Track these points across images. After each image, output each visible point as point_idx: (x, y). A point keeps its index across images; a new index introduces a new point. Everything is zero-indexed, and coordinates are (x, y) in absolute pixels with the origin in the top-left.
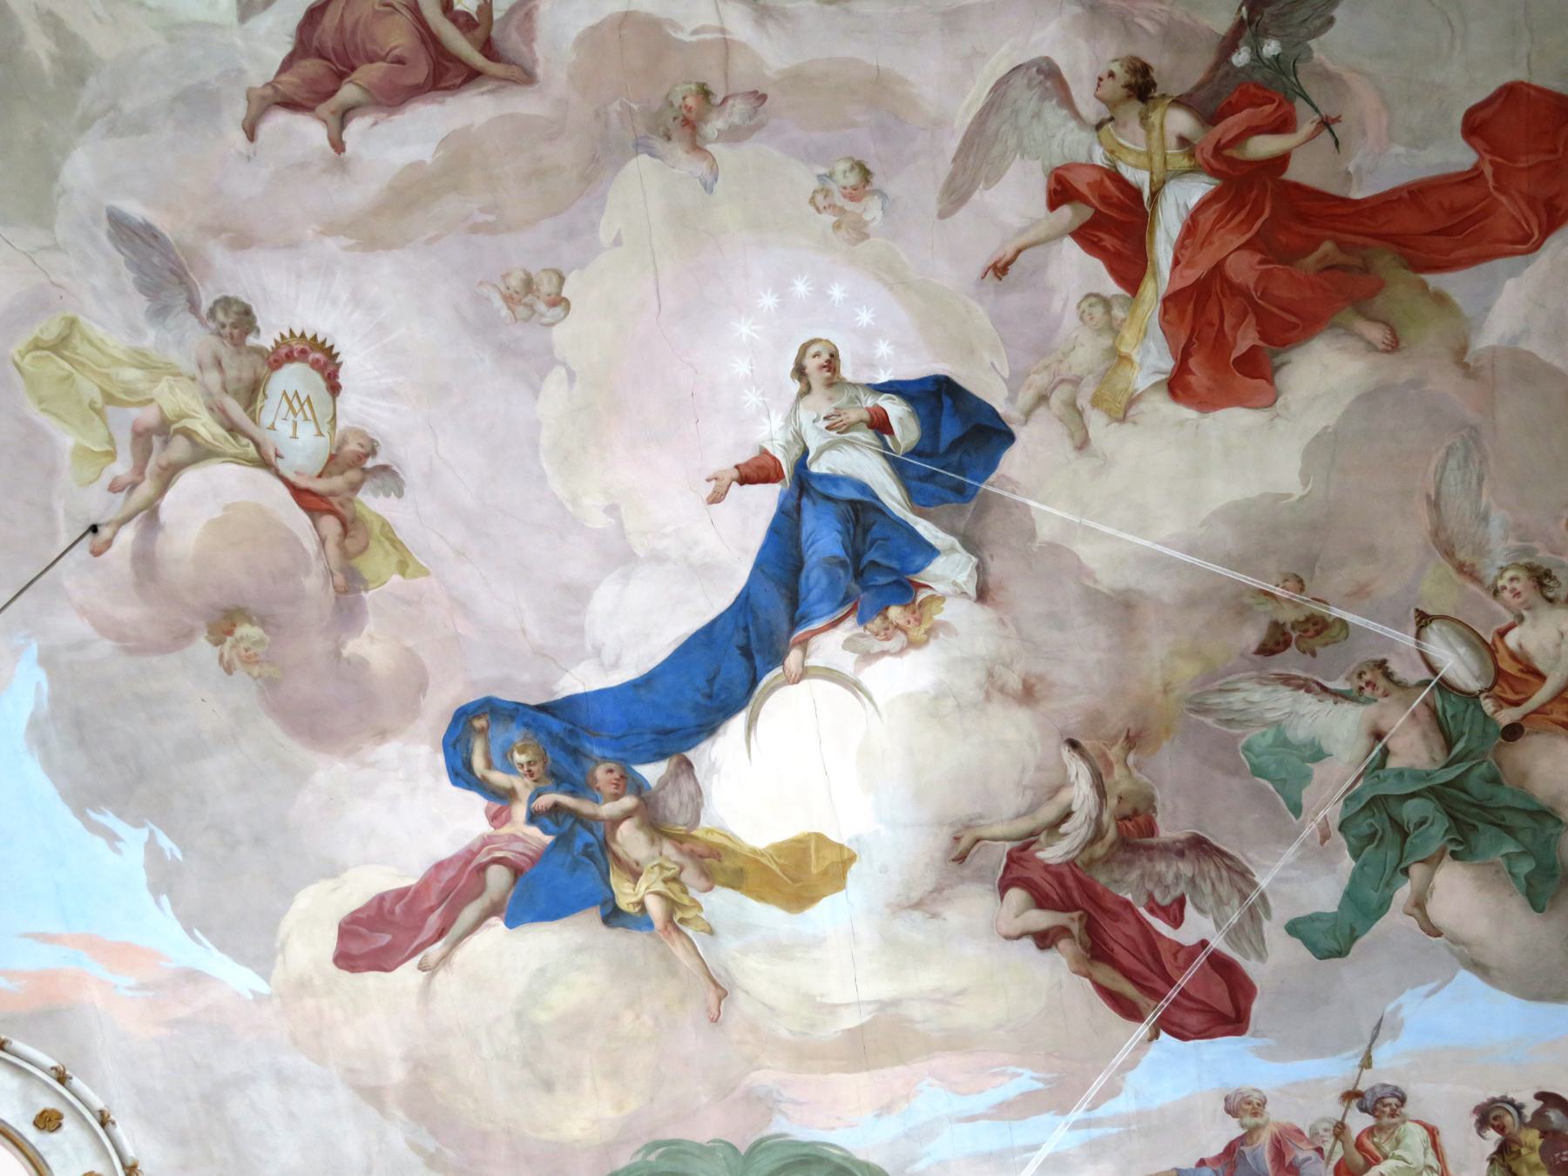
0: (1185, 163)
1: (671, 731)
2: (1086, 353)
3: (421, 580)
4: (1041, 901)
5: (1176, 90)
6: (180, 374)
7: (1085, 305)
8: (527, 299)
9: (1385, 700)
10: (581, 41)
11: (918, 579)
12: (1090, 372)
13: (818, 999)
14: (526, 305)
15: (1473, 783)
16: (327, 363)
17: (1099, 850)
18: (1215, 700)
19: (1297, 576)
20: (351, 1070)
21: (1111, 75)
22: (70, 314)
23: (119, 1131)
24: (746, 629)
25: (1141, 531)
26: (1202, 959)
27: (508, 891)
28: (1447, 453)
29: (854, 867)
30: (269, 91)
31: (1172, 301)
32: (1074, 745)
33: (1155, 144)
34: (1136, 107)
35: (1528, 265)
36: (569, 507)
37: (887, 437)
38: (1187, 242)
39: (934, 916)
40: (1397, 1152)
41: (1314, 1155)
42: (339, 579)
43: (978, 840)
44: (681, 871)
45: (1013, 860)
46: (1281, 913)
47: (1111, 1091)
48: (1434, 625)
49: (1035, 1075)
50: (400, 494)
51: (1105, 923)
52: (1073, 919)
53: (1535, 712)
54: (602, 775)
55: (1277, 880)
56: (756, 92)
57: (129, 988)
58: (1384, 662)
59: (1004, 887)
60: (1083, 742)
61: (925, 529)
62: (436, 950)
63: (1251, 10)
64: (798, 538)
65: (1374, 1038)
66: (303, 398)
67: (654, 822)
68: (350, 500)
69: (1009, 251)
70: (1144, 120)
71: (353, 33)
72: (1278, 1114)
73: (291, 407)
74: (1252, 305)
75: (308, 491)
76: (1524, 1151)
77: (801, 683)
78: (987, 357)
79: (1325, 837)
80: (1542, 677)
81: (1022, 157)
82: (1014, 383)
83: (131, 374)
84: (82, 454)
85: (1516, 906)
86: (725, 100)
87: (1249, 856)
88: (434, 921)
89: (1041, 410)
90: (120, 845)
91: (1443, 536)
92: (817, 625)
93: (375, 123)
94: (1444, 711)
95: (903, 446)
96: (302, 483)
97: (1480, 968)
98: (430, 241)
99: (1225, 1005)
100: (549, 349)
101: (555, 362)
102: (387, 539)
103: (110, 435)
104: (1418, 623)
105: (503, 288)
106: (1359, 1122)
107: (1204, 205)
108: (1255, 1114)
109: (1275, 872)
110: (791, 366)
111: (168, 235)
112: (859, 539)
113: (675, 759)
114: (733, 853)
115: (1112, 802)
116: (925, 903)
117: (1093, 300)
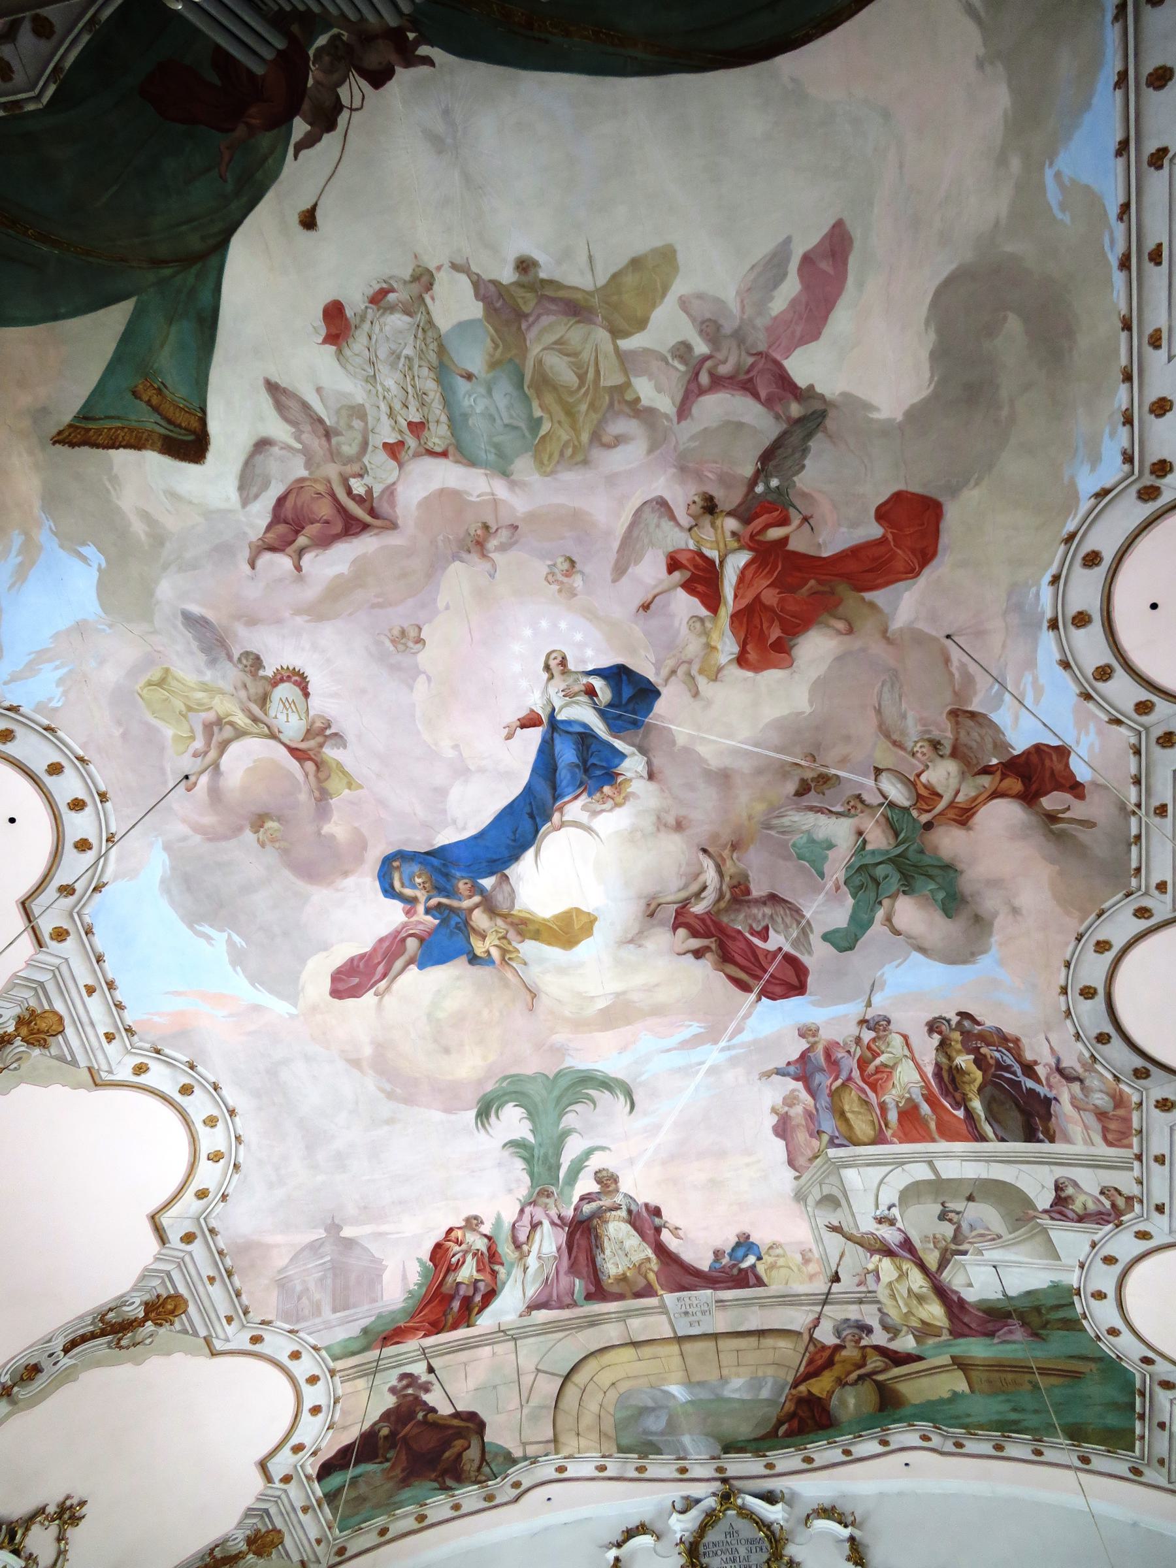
0: (736, 545)
2: (693, 647)
3: (360, 791)
4: (695, 934)
5: (728, 507)
7: (691, 622)
8: (403, 641)
9: (861, 815)
10: (420, 504)
11: (618, 770)
12: (696, 657)
15: (911, 854)
16: (301, 681)
17: (722, 904)
18: (775, 822)
20: (343, 1051)
21: (694, 502)
22: (165, 666)
23: (224, 1092)
24: (531, 804)
25: (729, 736)
26: (780, 957)
29: (597, 924)
30: (260, 543)
31: (735, 617)
32: (705, 851)
33: (720, 537)
34: (707, 520)
35: (914, 584)
36: (434, 747)
38: (741, 585)
41: (846, 1054)
42: (317, 794)
43: (659, 905)
44: (507, 932)
45: (678, 913)
47: (739, 1030)
48: (883, 774)
50: (345, 747)
51: (729, 943)
53: (940, 814)
54: (462, 886)
55: (815, 912)
58: (860, 795)
59: (675, 928)
60: (710, 849)
61: (618, 744)
62: (383, 984)
63: (762, 464)
65: (872, 991)
67: (491, 910)
68: (319, 752)
69: (650, 597)
70: (713, 525)
71: (302, 506)
72: (826, 1035)
73: (285, 706)
75: (297, 749)
77: (562, 829)
78: (643, 653)
79: (838, 888)
80: (941, 796)
82: (658, 666)
83: (200, 695)
84: (177, 738)
85: (938, 917)
86: (497, 530)
87: (799, 902)
88: (380, 969)
89: (673, 678)
90: (213, 942)
91: (883, 727)
92: (566, 799)
93: (317, 556)
96: (294, 745)
97: (922, 950)
98: (350, 614)
99: (794, 980)
100: (417, 666)
101: (419, 672)
103: (191, 727)
106: (867, 1036)
108: (814, 1036)
110: (542, 665)
112: (585, 752)
113: (499, 875)
114: (533, 921)
115: (727, 879)
116: (634, 940)
117: (694, 619)
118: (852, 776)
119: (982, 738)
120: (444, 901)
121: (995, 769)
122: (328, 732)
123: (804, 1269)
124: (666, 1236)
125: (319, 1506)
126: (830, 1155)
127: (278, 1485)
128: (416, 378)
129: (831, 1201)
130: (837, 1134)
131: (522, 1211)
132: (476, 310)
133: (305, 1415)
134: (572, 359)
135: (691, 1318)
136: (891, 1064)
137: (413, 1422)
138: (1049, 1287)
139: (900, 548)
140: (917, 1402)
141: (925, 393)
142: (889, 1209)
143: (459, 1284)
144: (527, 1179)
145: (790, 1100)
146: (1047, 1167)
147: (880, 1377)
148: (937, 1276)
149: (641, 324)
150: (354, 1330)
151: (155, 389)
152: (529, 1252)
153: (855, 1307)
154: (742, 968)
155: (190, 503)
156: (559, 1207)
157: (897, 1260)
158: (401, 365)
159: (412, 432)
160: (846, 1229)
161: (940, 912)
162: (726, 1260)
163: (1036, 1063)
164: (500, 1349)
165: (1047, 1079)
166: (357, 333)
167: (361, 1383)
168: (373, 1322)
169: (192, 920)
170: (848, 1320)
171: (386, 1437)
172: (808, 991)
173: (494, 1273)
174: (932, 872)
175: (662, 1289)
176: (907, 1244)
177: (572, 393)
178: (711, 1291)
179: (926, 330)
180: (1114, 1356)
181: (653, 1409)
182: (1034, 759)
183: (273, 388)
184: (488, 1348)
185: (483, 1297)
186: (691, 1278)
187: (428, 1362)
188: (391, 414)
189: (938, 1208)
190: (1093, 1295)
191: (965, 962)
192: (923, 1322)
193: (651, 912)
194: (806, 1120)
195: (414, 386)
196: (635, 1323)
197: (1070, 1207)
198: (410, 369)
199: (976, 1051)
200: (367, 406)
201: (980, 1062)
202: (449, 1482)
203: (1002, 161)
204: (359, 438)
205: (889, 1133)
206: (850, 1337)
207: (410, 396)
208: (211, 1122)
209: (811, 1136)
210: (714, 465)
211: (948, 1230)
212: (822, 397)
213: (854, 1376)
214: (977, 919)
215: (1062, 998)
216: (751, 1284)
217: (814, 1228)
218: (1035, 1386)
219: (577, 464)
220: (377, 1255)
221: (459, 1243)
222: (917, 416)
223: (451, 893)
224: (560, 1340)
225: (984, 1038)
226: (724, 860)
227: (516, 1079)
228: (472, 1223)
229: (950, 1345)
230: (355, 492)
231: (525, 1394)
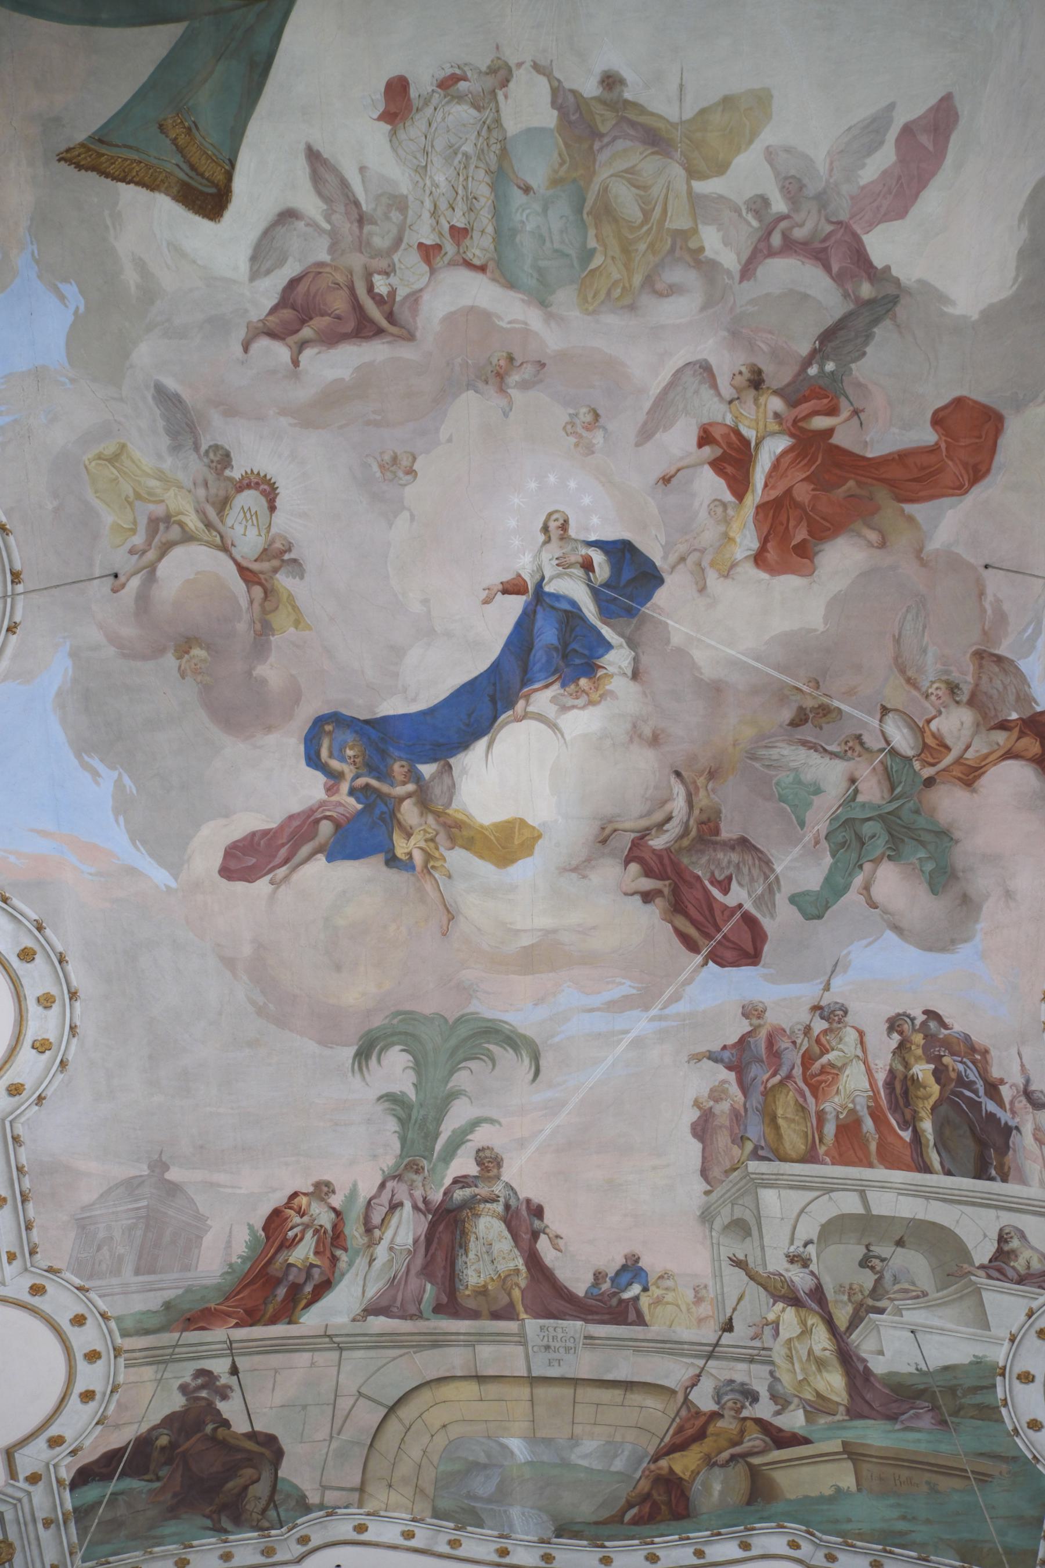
0: (776, 428)
2: (710, 535)
3: (307, 632)
4: (648, 873)
5: (776, 385)
6: (182, 488)
7: (712, 506)
8: (392, 469)
11: (599, 662)
13: (509, 926)
14: (391, 472)
16: (270, 492)
17: (686, 842)
18: (762, 752)
19: (816, 680)
21: (741, 373)
23: (70, 968)
24: (494, 684)
26: (738, 915)
27: (330, 838)
28: (907, 611)
29: (540, 842)
30: (260, 325)
31: (761, 508)
32: (678, 774)
33: (761, 415)
34: (752, 393)
37: (591, 574)
38: (773, 474)
39: (584, 877)
40: (840, 1046)
41: (790, 1045)
42: (258, 626)
43: (615, 831)
44: (437, 834)
45: (635, 844)
46: (787, 889)
47: (676, 998)
48: (890, 715)
49: (632, 984)
50: (302, 578)
51: (684, 889)
52: (665, 885)
53: (944, 770)
54: (398, 769)
56: (540, 362)
57: (91, 874)
58: (861, 735)
59: (627, 862)
60: (684, 773)
61: (607, 632)
62: (282, 872)
63: (821, 343)
64: (532, 630)
65: (833, 972)
66: (253, 512)
68: (271, 578)
69: (673, 470)
70: (756, 400)
72: (773, 1018)
75: (248, 569)
76: (913, 1047)
77: (523, 721)
79: (817, 843)
80: (948, 749)
81: (686, 416)
82: (667, 548)
83: (153, 483)
85: (922, 890)
86: (522, 364)
88: (283, 852)
89: (681, 566)
90: (99, 780)
91: (900, 661)
93: (319, 353)
94: (892, 768)
95: (599, 580)
96: (245, 563)
97: (897, 929)
99: (749, 948)
102: (290, 604)
103: (135, 518)
104: (882, 713)
105: (379, 459)
106: (819, 1025)
107: (784, 453)
108: (759, 1018)
109: (785, 863)
110: (541, 525)
111: (188, 402)
113: (442, 762)
114: (469, 827)
115: (696, 812)
116: (579, 869)
117: (717, 503)
118: (855, 713)
119: (1005, 688)
120: (374, 783)
121: (1012, 725)
122: (286, 557)
123: (694, 1309)
124: (543, 1244)
125: (65, 1523)
126: (750, 1169)
127: (22, 1484)
128: (470, 179)
129: (741, 1228)
130: (763, 1144)
131: (383, 1185)
132: (549, 118)
133: (74, 1398)
134: (642, 193)
135: (552, 1355)
136: (839, 1064)
137: (199, 1435)
138: (971, 1363)
139: (952, 460)
140: (792, 1497)
141: (1005, 294)
142: (805, 1246)
143: (290, 1265)
144: (397, 1145)
145: (717, 1094)
146: (992, 1212)
147: (756, 1461)
148: (845, 1337)
149: (721, 168)
150: (154, 1301)
151: (184, 127)
152: (381, 1239)
153: (742, 1366)
154: (694, 922)
155: (194, 262)
156: (427, 1188)
157: (803, 1312)
158: (456, 162)
159: (452, 236)
160: (751, 1265)
161: (925, 886)
162: (606, 1286)
163: (1002, 1082)
164: (320, 1358)
165: (1012, 1103)
166: (417, 117)
167: (148, 1373)
168: (178, 1297)
169: (82, 747)
170: (732, 1381)
171: (163, 1449)
172: (762, 962)
173: (334, 1260)
174: (927, 837)
175: (526, 1312)
176: (818, 1294)
179: (1019, 227)
180: (1030, 1457)
181: (485, 1467)
183: (313, 156)
184: (307, 1356)
185: (316, 1287)
186: (563, 1303)
187: (233, 1360)
188: (434, 213)
189: (860, 1251)
190: (1019, 1377)
191: (943, 949)
192: (819, 1395)
193: (604, 839)
194: (731, 1120)
195: (465, 188)
196: (485, 1351)
197: (1012, 1264)
198: (465, 167)
199: (937, 1060)
200: (411, 198)
201: (939, 1074)
202: (226, 1523)
204: (394, 231)
205: (822, 1150)
206: (730, 1404)
207: (459, 198)
208: (46, 1001)
209: (733, 1142)
210: (769, 336)
211: (868, 1280)
212: (897, 282)
213: (726, 1455)
216: (630, 1320)
217: (716, 1260)
218: (934, 1489)
219: (623, 307)
220: (201, 1210)
221: (301, 1213)
223: (385, 775)
224: (394, 1359)
225: (947, 1044)
226: (697, 788)
227: (410, 1016)
228: (322, 1190)
229: (845, 1428)
230: (376, 290)
231: (338, 1422)
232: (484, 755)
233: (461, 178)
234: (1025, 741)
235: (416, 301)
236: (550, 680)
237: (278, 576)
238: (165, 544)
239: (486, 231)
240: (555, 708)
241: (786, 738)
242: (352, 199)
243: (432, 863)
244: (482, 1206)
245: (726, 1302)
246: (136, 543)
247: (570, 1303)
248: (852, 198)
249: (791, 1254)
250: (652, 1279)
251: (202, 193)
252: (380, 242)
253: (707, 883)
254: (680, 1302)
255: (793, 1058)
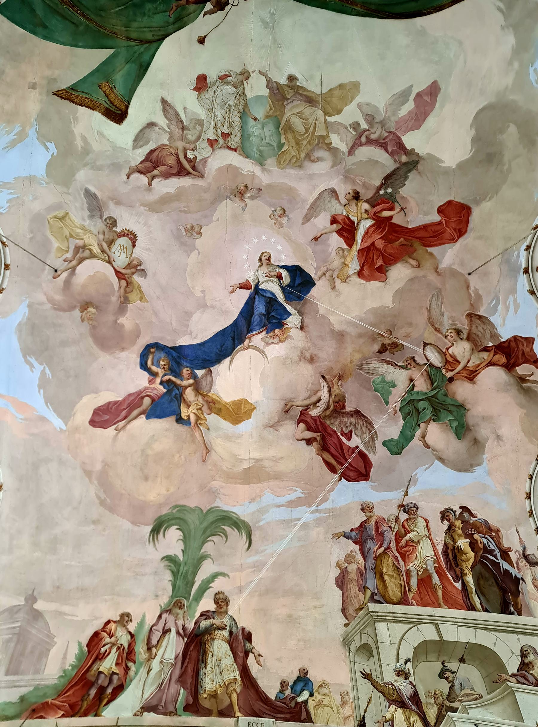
0: (366, 216)
1: (208, 360)
2: (337, 263)
4: (309, 429)
9: (414, 369)
10: (217, 170)
11: (284, 322)
13: (237, 456)
15: (440, 396)
16: (133, 238)
17: (328, 413)
20: (84, 463)
21: (349, 193)
24: (234, 332)
25: (347, 314)
26: (356, 452)
27: (149, 407)
28: (433, 296)
31: (360, 251)
32: (323, 377)
33: (359, 211)
34: (355, 201)
35: (454, 246)
39: (276, 430)
40: (415, 529)
42: (122, 299)
43: (292, 406)
44: (203, 406)
47: (325, 500)
48: (428, 346)
49: (301, 491)
50: (145, 278)
51: (328, 438)
52: (318, 436)
53: (457, 373)
54: (185, 372)
57: (21, 419)
58: (414, 357)
59: (298, 423)
61: (288, 307)
62: (122, 424)
63: (385, 181)
64: (253, 306)
65: (409, 485)
67: (197, 390)
70: (356, 205)
72: (378, 512)
74: (381, 253)
75: (120, 272)
76: (456, 529)
79: (395, 413)
80: (460, 363)
82: (317, 269)
83: (79, 231)
84: (59, 249)
85: (452, 437)
86: (251, 189)
87: (372, 418)
88: (124, 413)
89: (324, 277)
90: (34, 369)
91: (431, 320)
92: (254, 333)
94: (431, 373)
96: (118, 269)
97: (441, 459)
98: (168, 212)
99: (363, 470)
102: (139, 289)
104: (424, 346)
106: (403, 516)
107: (370, 227)
108: (370, 512)
112: (270, 308)
113: (207, 369)
114: (219, 403)
115: (333, 397)
116: (274, 426)
118: (410, 346)
119: (484, 331)
120: (173, 378)
121: (490, 348)
122: (139, 268)
124: (251, 660)
128: (231, 114)
131: (160, 617)
132: (266, 92)
134: (305, 121)
136: (416, 541)
139: (449, 228)
142: (406, 663)
143: (100, 673)
145: (349, 559)
149: (339, 112)
151: (110, 87)
152: (156, 655)
154: (333, 456)
155: (108, 140)
156: (186, 619)
157: (408, 712)
158: (225, 108)
160: (374, 677)
161: (454, 435)
163: (510, 549)
165: (517, 563)
169: (26, 352)
172: (370, 479)
173: (127, 669)
174: (452, 408)
175: (240, 711)
176: (415, 697)
177: (301, 135)
178: (273, 720)
182: (513, 344)
183: (164, 102)
189: (439, 667)
191: (467, 470)
200: (205, 121)
201: (473, 545)
203: (510, 63)
204: (198, 133)
205: (410, 596)
211: (444, 687)
212: (418, 155)
214: (476, 442)
215: (527, 502)
217: (353, 673)
221: (111, 635)
222: (462, 166)
223: (179, 375)
226: (333, 384)
227: (182, 508)
230: (188, 157)
232: (228, 367)
233: (227, 114)
234: (497, 357)
235: (205, 162)
236: (261, 330)
237: (134, 276)
238: (81, 258)
239: (237, 135)
240: (263, 343)
241: (377, 359)
242: (180, 120)
243: (199, 422)
244: (216, 632)
245: (360, 704)
246: (68, 257)
247: (266, 704)
248: (396, 122)
249: (398, 669)
250: (315, 688)
251: (115, 113)
252: (190, 137)
253: (339, 434)
254: (332, 705)
255: (390, 536)
